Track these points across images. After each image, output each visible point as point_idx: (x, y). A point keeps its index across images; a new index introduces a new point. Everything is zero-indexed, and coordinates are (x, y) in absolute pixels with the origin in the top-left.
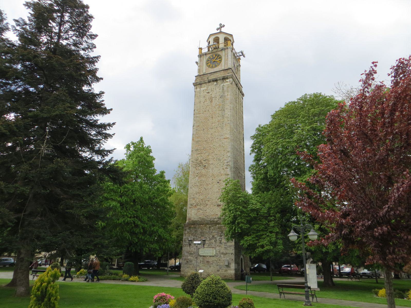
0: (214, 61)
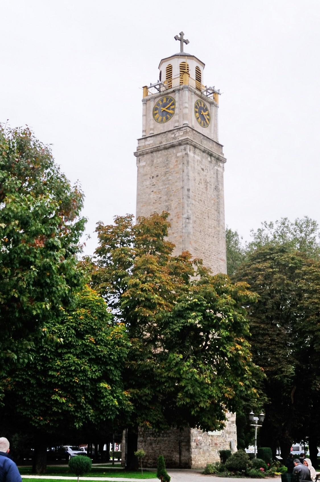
0: (164, 110)
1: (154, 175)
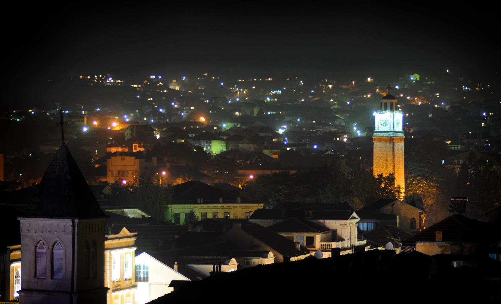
1: (381, 146)
